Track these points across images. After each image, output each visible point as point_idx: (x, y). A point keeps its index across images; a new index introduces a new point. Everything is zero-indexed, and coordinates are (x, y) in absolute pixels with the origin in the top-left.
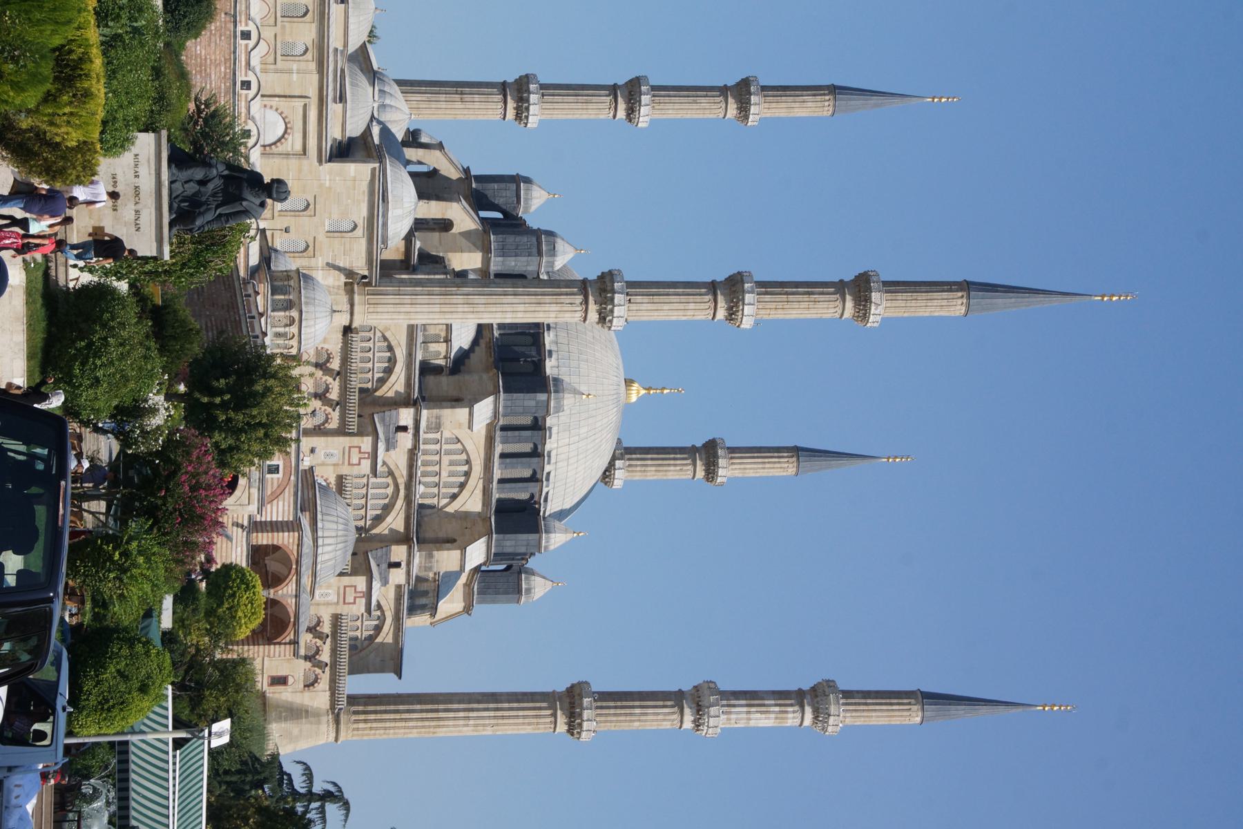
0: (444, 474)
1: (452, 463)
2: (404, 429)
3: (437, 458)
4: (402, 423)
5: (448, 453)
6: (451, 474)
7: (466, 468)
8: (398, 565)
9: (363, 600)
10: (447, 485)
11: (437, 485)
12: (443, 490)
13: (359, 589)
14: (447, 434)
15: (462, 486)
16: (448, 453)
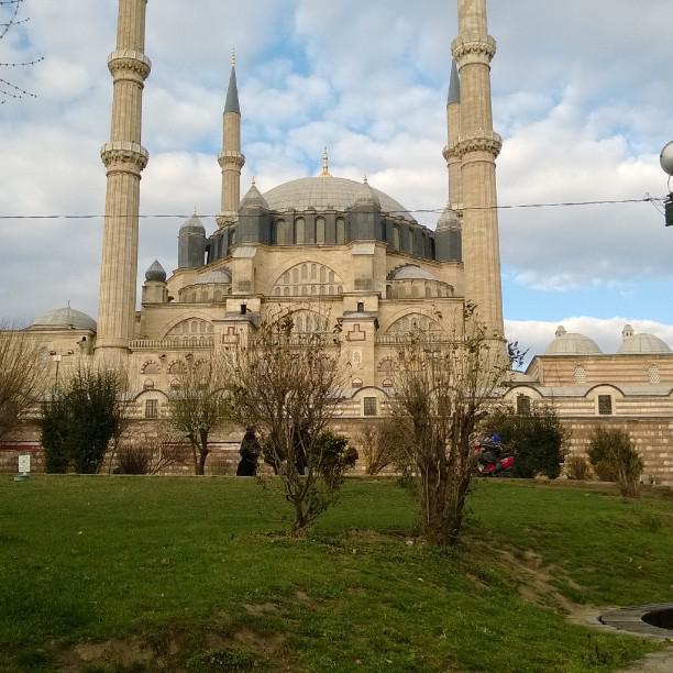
0: (313, 282)
1: (304, 277)
2: (244, 307)
3: (300, 288)
4: (239, 309)
5: (296, 279)
6: (314, 276)
7: (309, 265)
8: (360, 304)
9: (362, 324)
10: (322, 278)
11: (322, 286)
12: (327, 281)
13: (352, 329)
14: (281, 281)
15: (323, 267)
16: (296, 279)
